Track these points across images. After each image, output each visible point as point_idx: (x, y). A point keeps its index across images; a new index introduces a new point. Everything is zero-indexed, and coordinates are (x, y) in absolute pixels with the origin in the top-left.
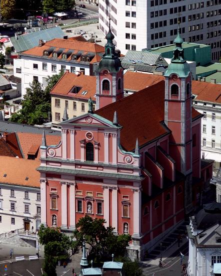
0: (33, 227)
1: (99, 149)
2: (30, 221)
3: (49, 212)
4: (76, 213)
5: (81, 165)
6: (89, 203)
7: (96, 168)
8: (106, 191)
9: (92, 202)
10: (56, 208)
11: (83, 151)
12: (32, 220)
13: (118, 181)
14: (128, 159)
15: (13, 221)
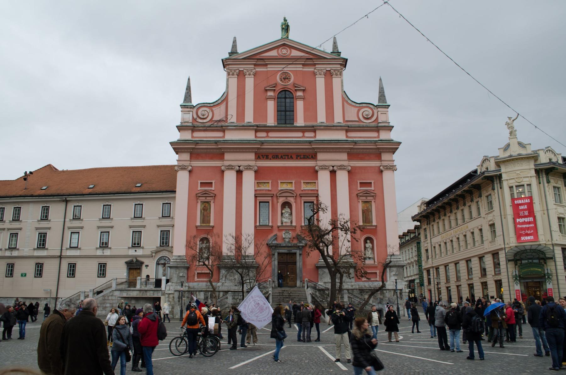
0: (148, 276)
1: (303, 98)
2: (142, 263)
3: (194, 232)
4: (256, 227)
5: (268, 129)
6: (286, 204)
7: (300, 134)
8: (324, 178)
9: (292, 200)
10: (210, 223)
11: (271, 106)
12: (146, 261)
13: (349, 154)
14: (367, 113)
15: (102, 270)
